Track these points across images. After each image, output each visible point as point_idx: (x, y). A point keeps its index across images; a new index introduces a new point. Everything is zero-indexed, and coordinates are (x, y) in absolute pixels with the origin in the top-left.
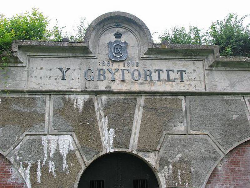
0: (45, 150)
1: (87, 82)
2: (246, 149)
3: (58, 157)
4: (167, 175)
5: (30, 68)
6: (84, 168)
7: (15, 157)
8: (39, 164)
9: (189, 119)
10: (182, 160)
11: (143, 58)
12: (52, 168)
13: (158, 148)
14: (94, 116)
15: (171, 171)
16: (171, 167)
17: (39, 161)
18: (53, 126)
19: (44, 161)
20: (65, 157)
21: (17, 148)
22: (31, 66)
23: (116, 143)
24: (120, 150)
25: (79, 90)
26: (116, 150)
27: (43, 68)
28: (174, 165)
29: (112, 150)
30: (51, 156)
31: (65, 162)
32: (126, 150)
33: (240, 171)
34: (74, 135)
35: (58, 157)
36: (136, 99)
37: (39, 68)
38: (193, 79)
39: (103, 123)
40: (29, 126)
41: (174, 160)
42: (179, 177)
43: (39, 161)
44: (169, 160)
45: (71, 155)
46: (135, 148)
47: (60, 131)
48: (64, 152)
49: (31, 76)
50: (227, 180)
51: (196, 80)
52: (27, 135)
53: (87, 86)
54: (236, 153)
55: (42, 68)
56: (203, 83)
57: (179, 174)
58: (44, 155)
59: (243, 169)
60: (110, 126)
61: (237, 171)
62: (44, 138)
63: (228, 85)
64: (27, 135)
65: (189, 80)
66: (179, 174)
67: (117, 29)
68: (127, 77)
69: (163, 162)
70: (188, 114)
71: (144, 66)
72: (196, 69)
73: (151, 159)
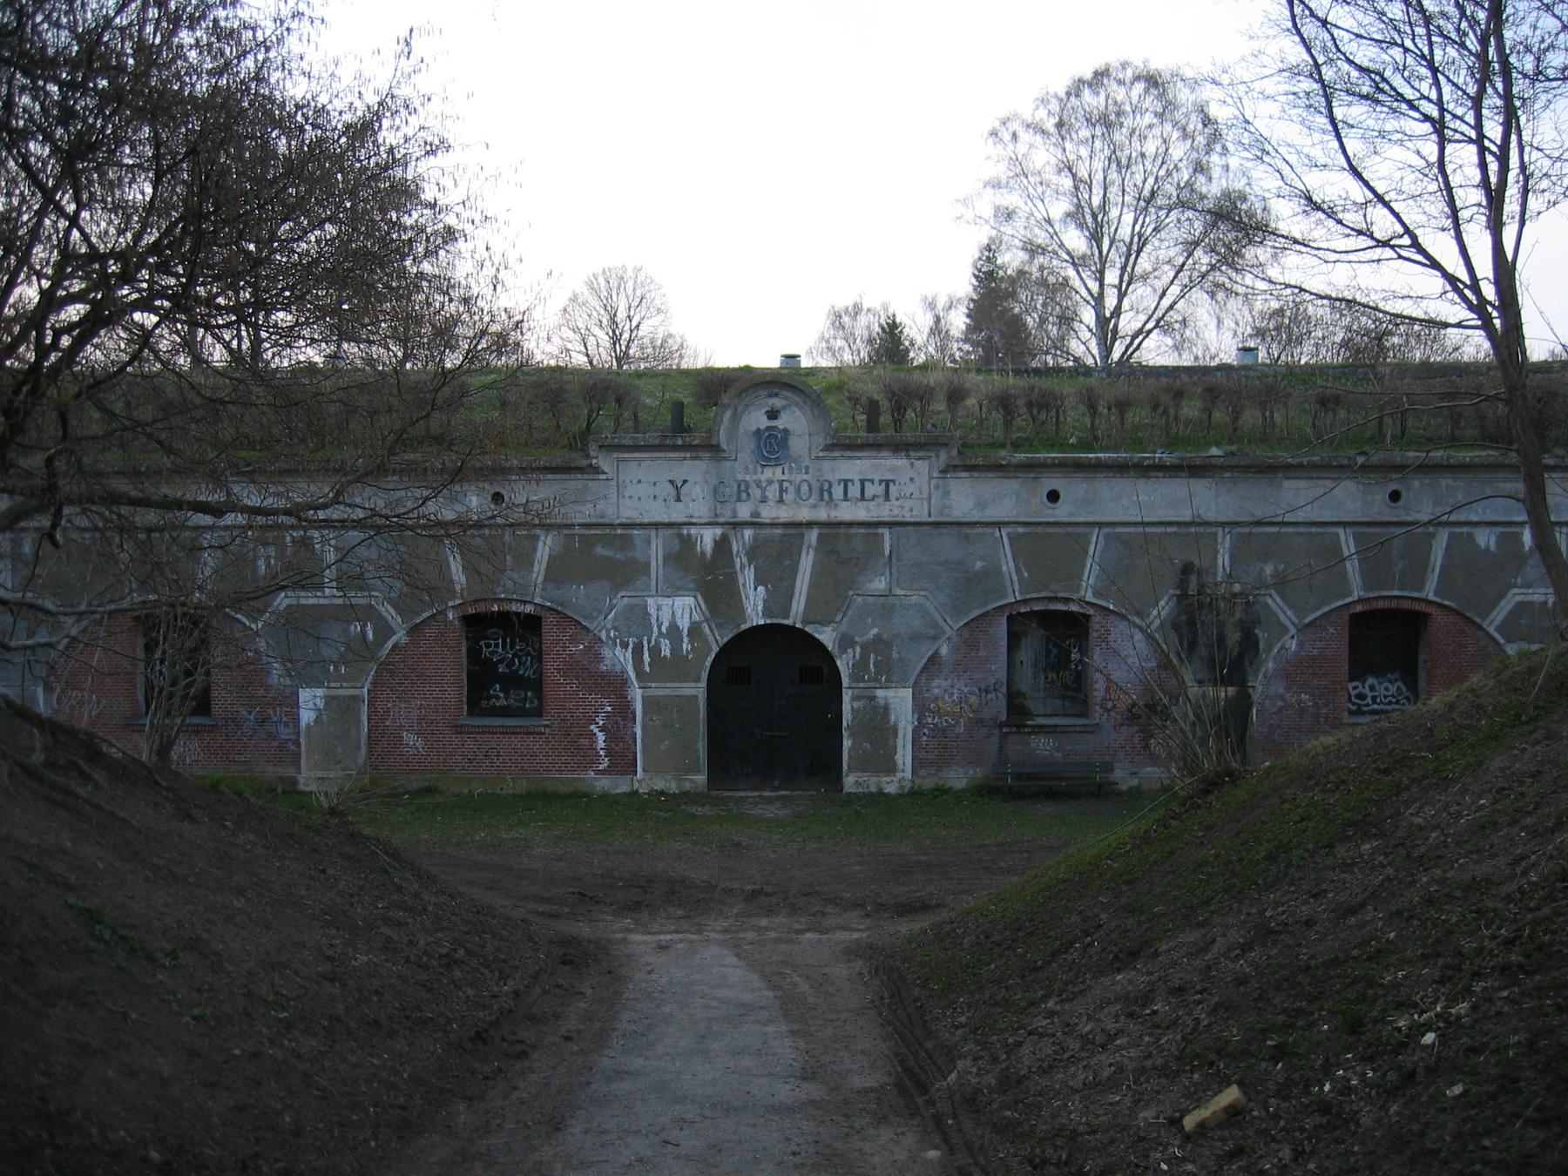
0: (654, 621)
6: (715, 649)
7: (608, 632)
8: (645, 643)
10: (878, 639)
12: (666, 651)
14: (733, 565)
16: (858, 650)
20: (686, 630)
23: (767, 612)
24: (775, 621)
26: (768, 621)
28: (864, 647)
30: (664, 630)
31: (686, 640)
32: (785, 622)
34: (700, 597)
35: (674, 629)
36: (803, 535)
39: (747, 577)
41: (864, 639)
44: (857, 639)
45: (694, 630)
46: (799, 619)
47: (675, 590)
48: (684, 624)
55: (640, 481)
56: (925, 503)
60: (759, 581)
69: (846, 642)
72: (914, 475)
73: (826, 636)
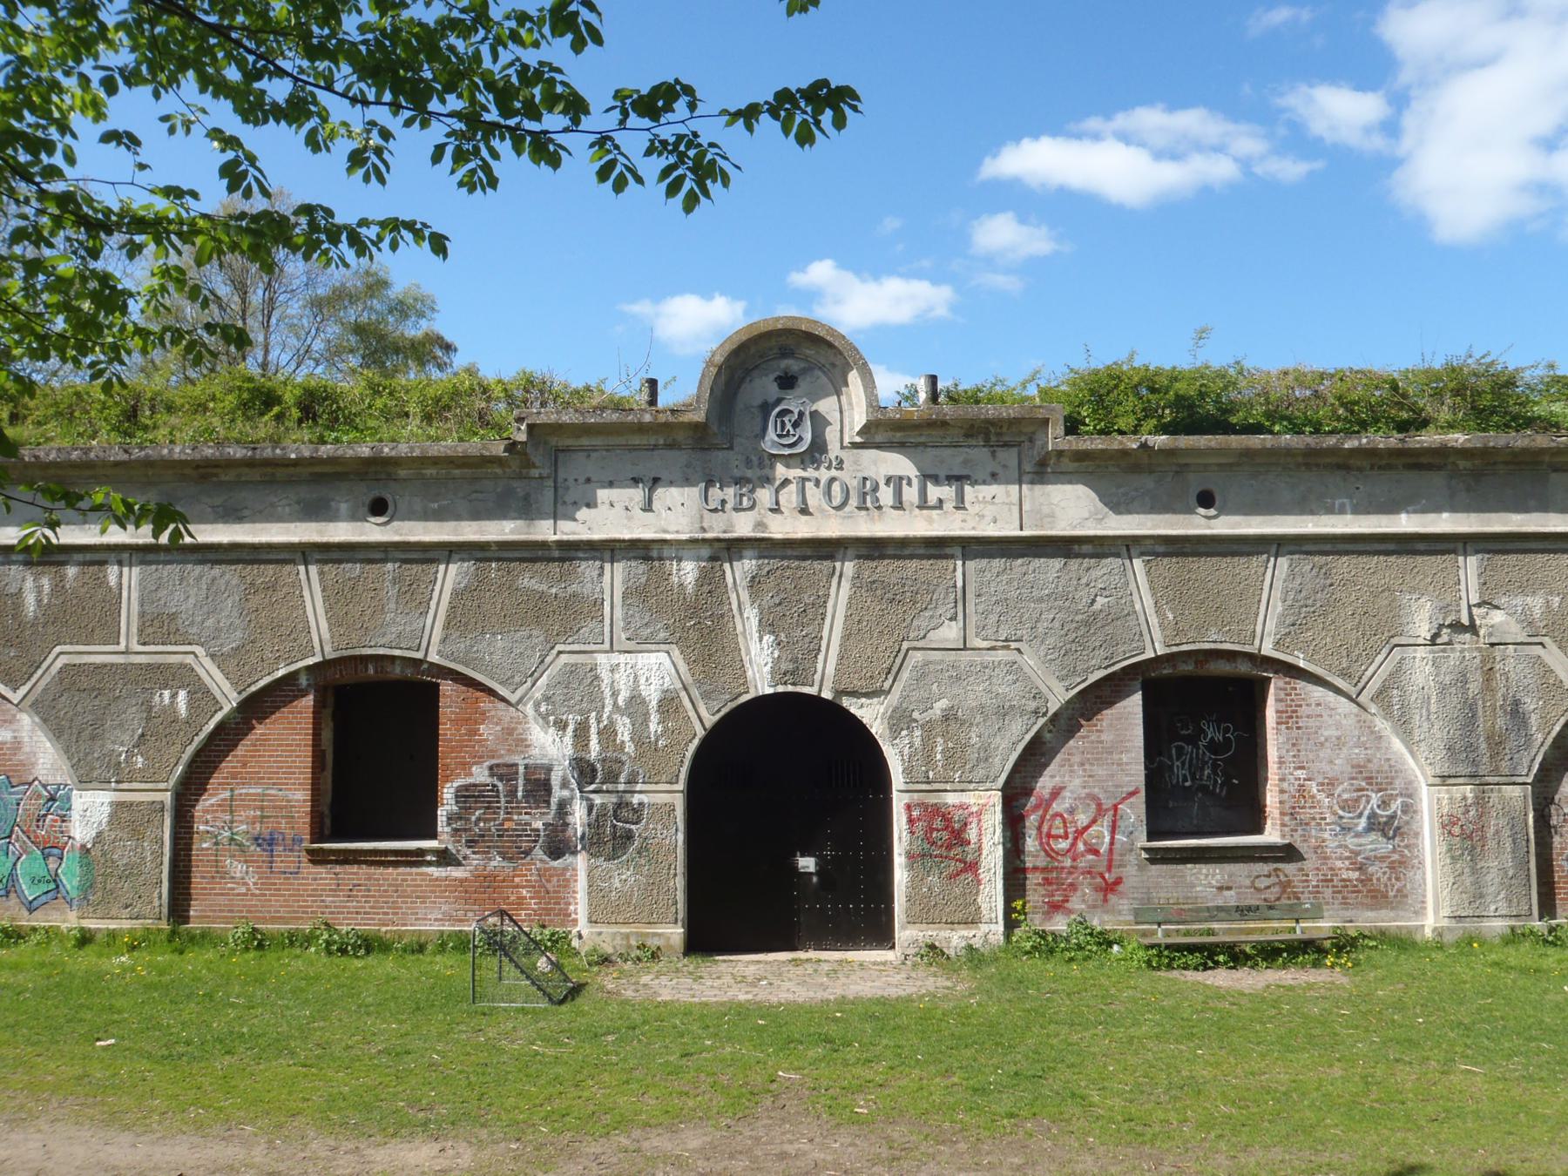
0: (607, 693)
1: (707, 514)
2: (1125, 686)
3: (636, 704)
4: (906, 751)
5: (560, 480)
6: (701, 733)
7: (537, 705)
8: (592, 721)
9: (970, 608)
10: (948, 717)
11: (855, 445)
12: (624, 732)
13: (887, 685)
14: (723, 601)
15: (917, 742)
16: (918, 733)
17: (594, 714)
18: (625, 629)
19: (605, 716)
20: (654, 703)
21: (539, 683)
22: (561, 475)
23: (779, 675)
24: (790, 688)
25: (684, 537)
26: (780, 689)
27: (593, 479)
28: (928, 727)
29: (770, 691)
30: (621, 702)
31: (654, 718)
32: (806, 690)
33: (1102, 742)
34: (676, 652)
35: (636, 704)
37: (582, 479)
38: (989, 498)
39: (748, 620)
40: (568, 632)
41: (927, 716)
42: (939, 756)
43: (594, 714)
44: (916, 715)
45: (668, 704)
46: (828, 684)
47: (641, 642)
48: (652, 694)
49: (565, 503)
50: (1064, 766)
51: (996, 500)
52: (560, 652)
53: (705, 525)
54: (1097, 697)
55: (588, 480)
56: (1016, 509)
57: (939, 749)
58: (602, 699)
59: (1111, 737)
60: (767, 625)
61: (1092, 742)
62: (601, 659)
63: (1087, 515)
64: (560, 652)
65: (979, 502)
66: (939, 749)
67: (784, 363)
68: (814, 496)
69: (900, 721)
70: (970, 596)
71: (855, 467)
72: (999, 470)
73: (871, 714)
